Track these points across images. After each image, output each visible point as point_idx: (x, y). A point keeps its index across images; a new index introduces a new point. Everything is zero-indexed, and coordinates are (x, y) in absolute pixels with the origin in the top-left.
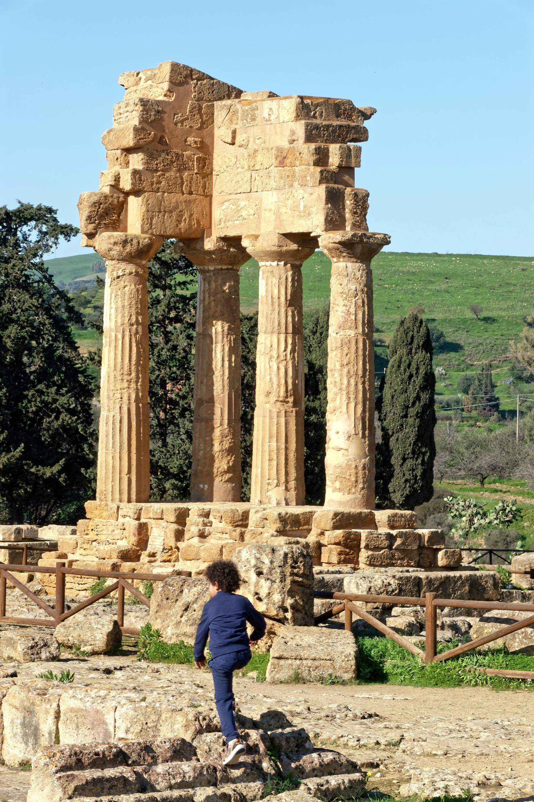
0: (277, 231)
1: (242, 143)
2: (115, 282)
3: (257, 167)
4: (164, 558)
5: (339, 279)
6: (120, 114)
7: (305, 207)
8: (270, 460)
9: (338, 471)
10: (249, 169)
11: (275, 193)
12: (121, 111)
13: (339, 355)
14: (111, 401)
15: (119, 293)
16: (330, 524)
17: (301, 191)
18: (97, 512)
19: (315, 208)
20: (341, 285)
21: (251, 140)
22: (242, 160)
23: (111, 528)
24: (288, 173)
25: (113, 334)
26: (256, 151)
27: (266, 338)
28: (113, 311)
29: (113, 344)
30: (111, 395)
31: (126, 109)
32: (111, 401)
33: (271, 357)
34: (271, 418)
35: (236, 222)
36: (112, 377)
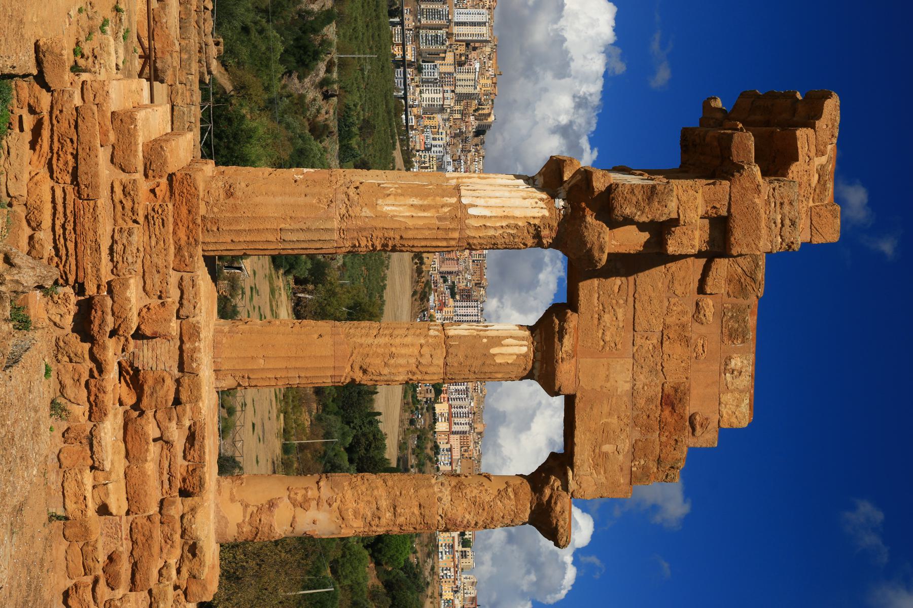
0: (578, 395)
1: (702, 312)
2: (532, 230)
3: (666, 343)
4: (124, 364)
5: (510, 515)
6: (782, 204)
7: (606, 455)
9: (266, 529)
10: (666, 326)
11: (628, 387)
12: (787, 208)
13: (413, 520)
14: (356, 235)
17: (626, 446)
18: (184, 210)
19: (604, 480)
20: (503, 517)
21: (703, 330)
22: (680, 308)
23: (161, 263)
24: (652, 416)
26: (687, 341)
28: (491, 233)
29: (441, 234)
30: (365, 234)
31: (787, 222)
33: (414, 374)
35: (597, 295)
36: (391, 234)
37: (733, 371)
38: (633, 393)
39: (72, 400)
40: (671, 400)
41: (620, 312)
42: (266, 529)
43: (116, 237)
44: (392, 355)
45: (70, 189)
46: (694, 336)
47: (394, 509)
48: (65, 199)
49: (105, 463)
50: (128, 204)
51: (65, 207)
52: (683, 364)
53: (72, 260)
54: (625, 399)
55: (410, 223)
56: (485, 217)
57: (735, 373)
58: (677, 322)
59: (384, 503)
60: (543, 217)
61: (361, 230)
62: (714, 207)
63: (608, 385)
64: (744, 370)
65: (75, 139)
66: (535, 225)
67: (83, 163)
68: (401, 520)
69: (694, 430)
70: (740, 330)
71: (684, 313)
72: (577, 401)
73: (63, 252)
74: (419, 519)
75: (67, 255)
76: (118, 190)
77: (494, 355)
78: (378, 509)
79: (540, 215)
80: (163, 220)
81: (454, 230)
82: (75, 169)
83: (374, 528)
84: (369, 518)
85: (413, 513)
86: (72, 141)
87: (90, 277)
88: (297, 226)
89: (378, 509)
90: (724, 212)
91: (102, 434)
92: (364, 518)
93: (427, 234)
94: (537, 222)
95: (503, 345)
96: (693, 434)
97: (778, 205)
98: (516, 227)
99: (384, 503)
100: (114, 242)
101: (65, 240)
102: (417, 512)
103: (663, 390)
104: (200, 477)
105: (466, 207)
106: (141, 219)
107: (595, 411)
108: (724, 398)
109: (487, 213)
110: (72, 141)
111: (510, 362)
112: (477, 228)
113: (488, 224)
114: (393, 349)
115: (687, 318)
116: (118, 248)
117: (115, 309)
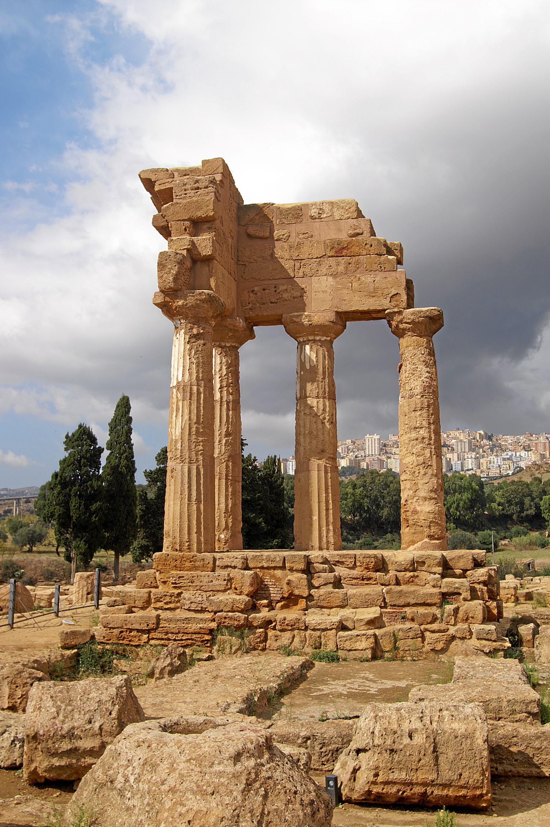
0: (336, 310)
3: (301, 257)
5: (421, 350)
6: (185, 190)
8: (327, 510)
9: (432, 516)
11: (330, 279)
12: (188, 187)
13: (425, 415)
15: (200, 349)
16: (470, 565)
21: (293, 235)
23: (206, 580)
25: (195, 388)
27: (318, 402)
29: (195, 397)
30: (193, 447)
31: (196, 185)
32: (194, 452)
34: (326, 472)
37: (319, 213)
38: (334, 276)
39: (290, 641)
40: (340, 250)
41: (282, 288)
42: (432, 516)
43: (186, 607)
44: (311, 433)
45: (152, 635)
46: (298, 240)
47: (417, 428)
48: (158, 639)
49: (334, 621)
50: (168, 599)
51: (162, 639)
52: (315, 245)
53: (194, 636)
54: (338, 279)
55: (186, 417)
56: (183, 370)
57: (320, 212)
58: (288, 251)
59: (414, 435)
60: (185, 333)
61: (190, 449)
62: (185, 229)
63: (329, 291)
64: (319, 207)
65: (120, 630)
66: (189, 338)
67: (134, 625)
68: (425, 423)
69: (358, 234)
70: (293, 212)
71: (282, 247)
72: (340, 310)
73: (190, 642)
74: (425, 411)
75: (192, 639)
76: (159, 604)
77: (310, 366)
78: (417, 439)
79: (183, 335)
80: (180, 577)
81: (191, 389)
82: (138, 631)
83: (432, 442)
84: (424, 445)
85: (420, 415)
86: (122, 632)
87: (205, 626)
88: (186, 490)
89: (417, 439)
90: (187, 223)
91: (314, 622)
92: (423, 449)
93: (194, 406)
94: (188, 337)
95: (305, 361)
96: (362, 234)
97: (186, 192)
98: (190, 350)
99: (414, 435)
100: (189, 610)
101: (182, 640)
102: (419, 413)
103: (332, 257)
104: (364, 557)
105: (178, 383)
106: (177, 591)
107: (346, 298)
108: (337, 217)
109: (181, 368)
110: (122, 632)
111: (315, 356)
112: (190, 374)
113: (188, 368)
114: (307, 432)
115: (286, 245)
116: (193, 607)
117: (227, 610)
